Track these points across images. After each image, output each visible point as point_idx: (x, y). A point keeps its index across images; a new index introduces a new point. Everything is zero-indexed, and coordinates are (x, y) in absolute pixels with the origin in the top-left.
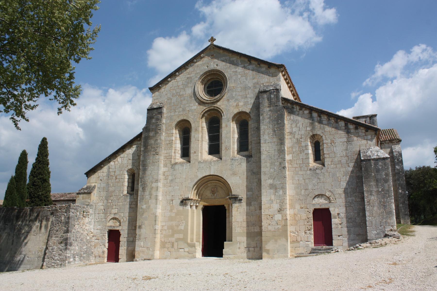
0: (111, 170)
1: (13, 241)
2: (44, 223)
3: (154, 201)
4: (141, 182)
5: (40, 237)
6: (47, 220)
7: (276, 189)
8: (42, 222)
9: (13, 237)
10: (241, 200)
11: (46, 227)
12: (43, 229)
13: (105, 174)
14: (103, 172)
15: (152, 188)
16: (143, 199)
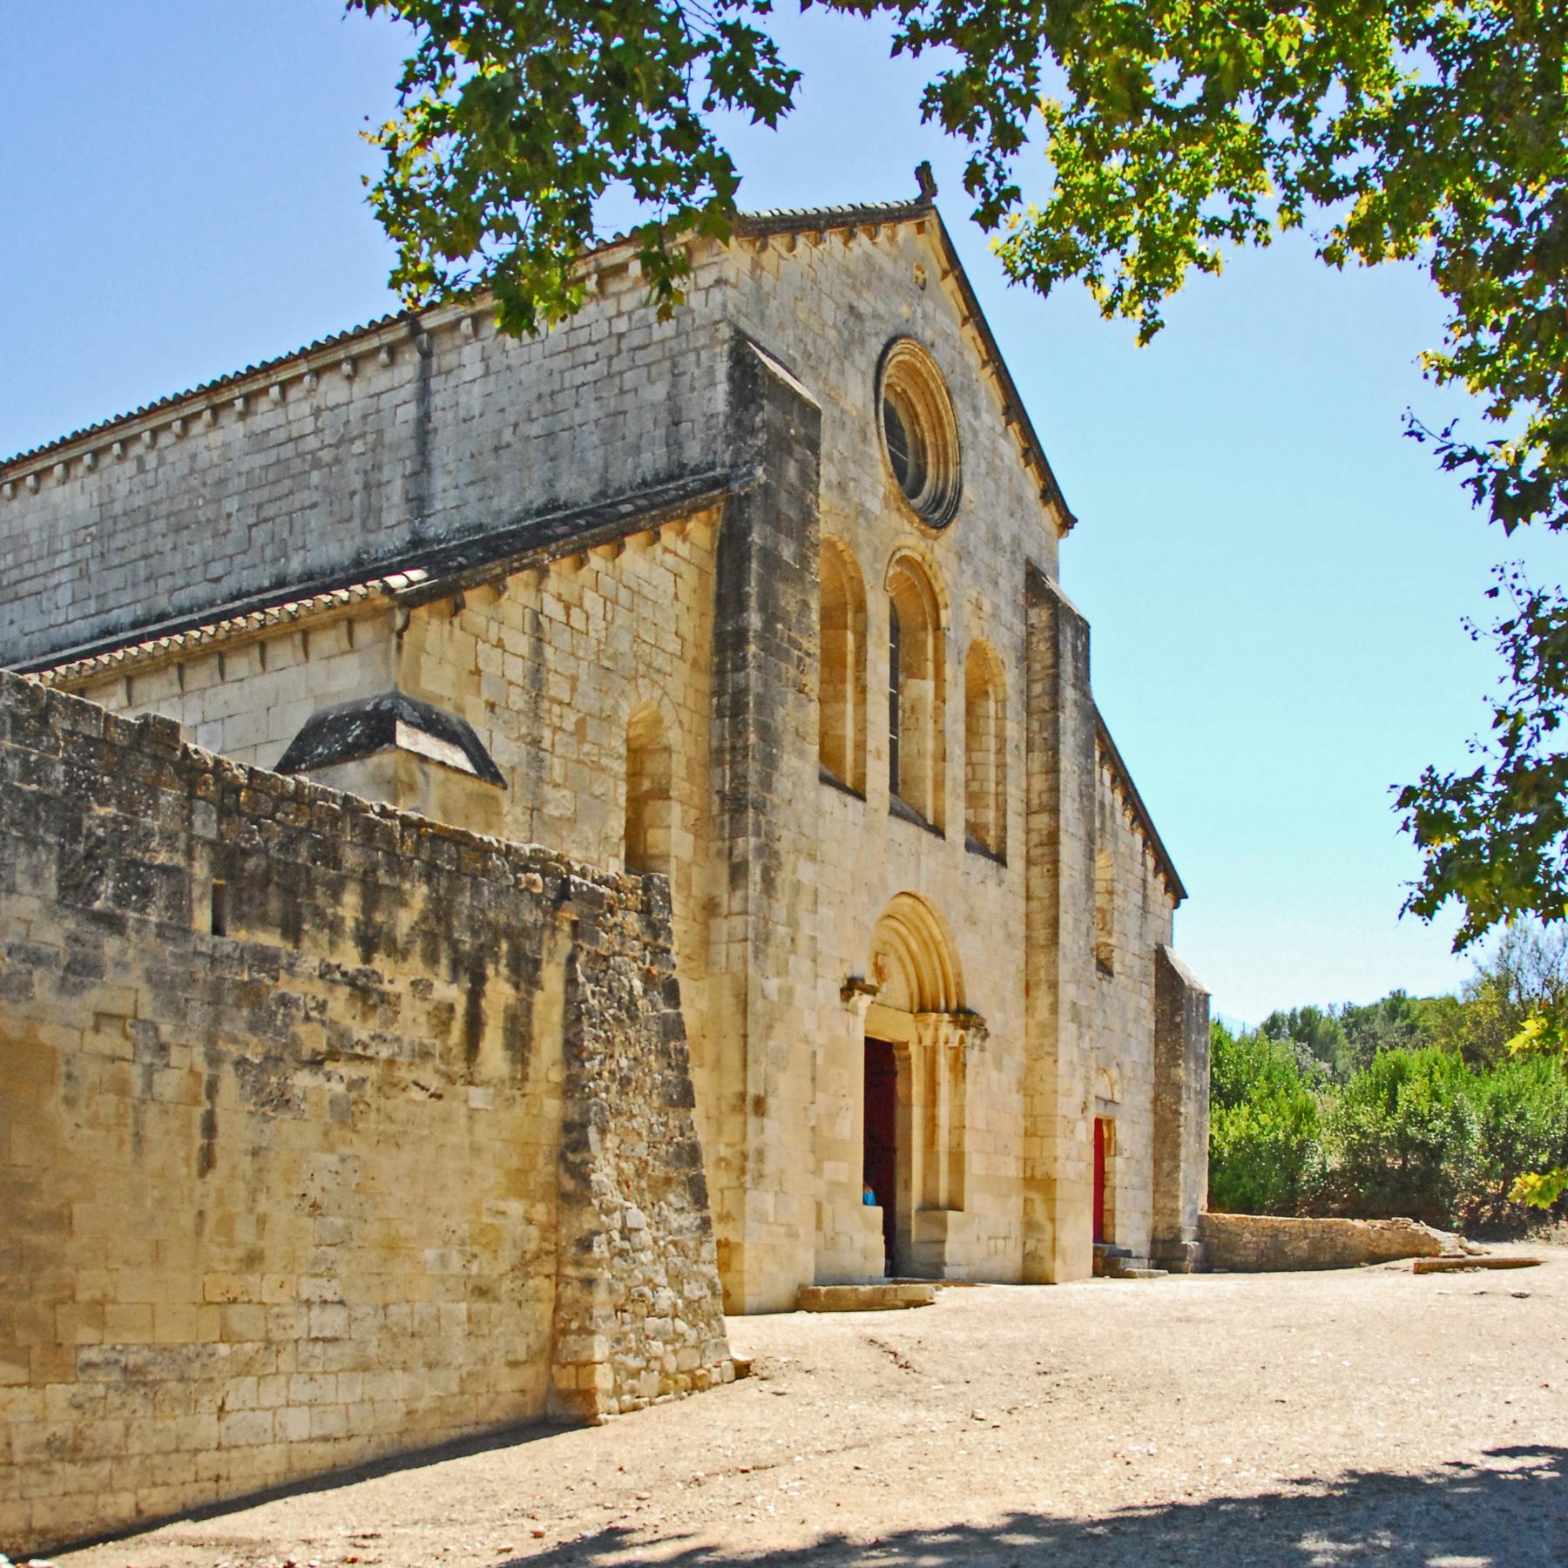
0: (548, 651)
1: (210, 1128)
2: (499, 992)
3: (806, 966)
4: (757, 834)
5: (472, 1114)
6: (525, 973)
7: (1080, 1025)
8: (478, 980)
9: (212, 1089)
10: (986, 1036)
11: (519, 1039)
12: (494, 1054)
13: (517, 671)
14: (500, 644)
15: (797, 887)
16: (767, 941)
